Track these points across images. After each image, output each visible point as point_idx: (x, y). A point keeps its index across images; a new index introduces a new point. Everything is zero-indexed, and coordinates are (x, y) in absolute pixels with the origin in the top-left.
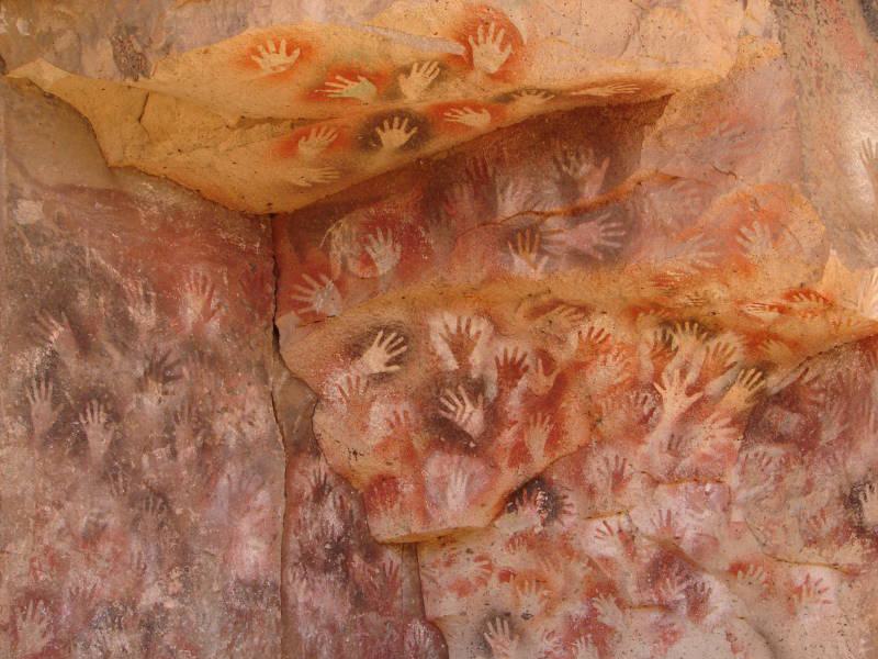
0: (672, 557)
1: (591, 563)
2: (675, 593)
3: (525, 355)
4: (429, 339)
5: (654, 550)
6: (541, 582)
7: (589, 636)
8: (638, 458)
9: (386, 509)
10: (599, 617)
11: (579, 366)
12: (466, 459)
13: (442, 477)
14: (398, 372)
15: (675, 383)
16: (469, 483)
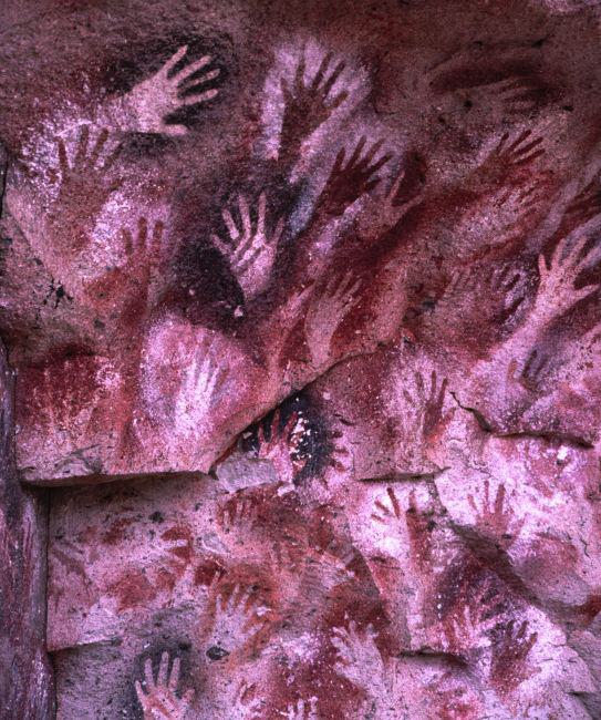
0: (478, 569)
1: (357, 564)
2: (477, 636)
3: (385, 159)
4: (259, 83)
5: (455, 552)
6: (261, 589)
7: (314, 699)
8: (469, 384)
9: (60, 418)
10: (338, 665)
11: (460, 199)
12: (217, 340)
13: (175, 368)
14: (180, 140)
15: (568, 262)
16: (218, 388)
